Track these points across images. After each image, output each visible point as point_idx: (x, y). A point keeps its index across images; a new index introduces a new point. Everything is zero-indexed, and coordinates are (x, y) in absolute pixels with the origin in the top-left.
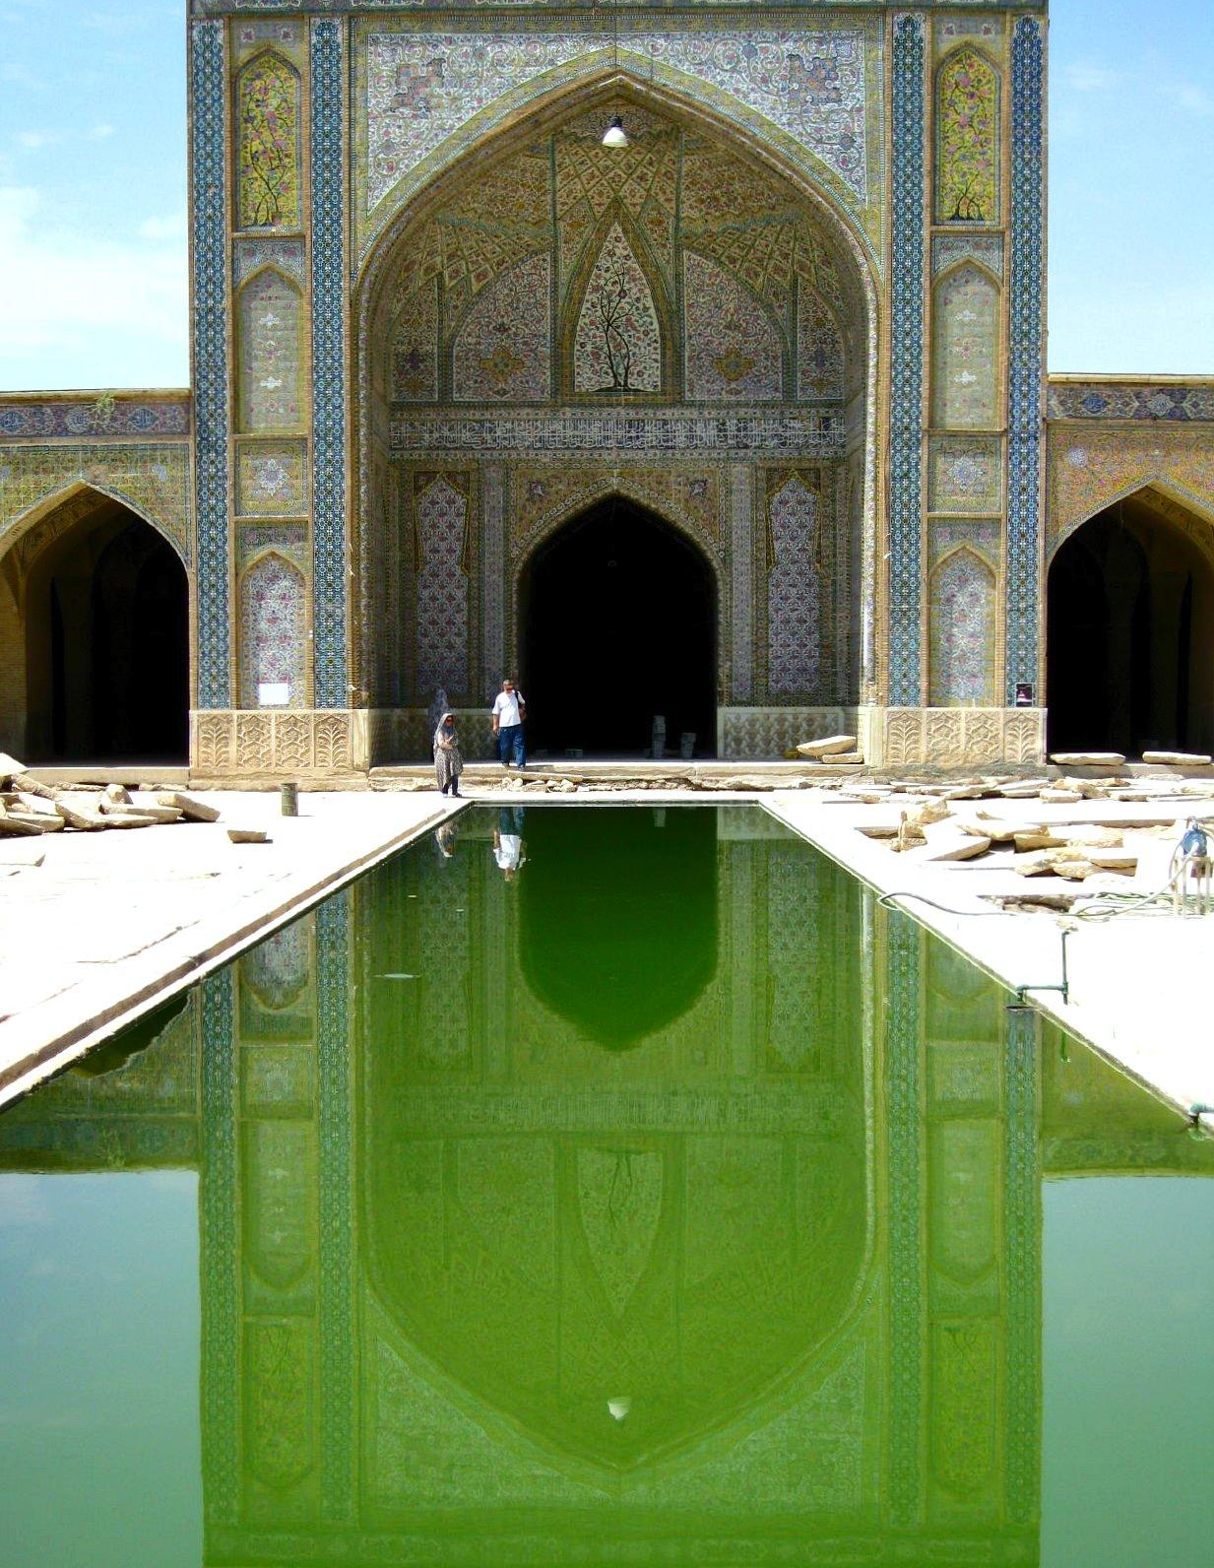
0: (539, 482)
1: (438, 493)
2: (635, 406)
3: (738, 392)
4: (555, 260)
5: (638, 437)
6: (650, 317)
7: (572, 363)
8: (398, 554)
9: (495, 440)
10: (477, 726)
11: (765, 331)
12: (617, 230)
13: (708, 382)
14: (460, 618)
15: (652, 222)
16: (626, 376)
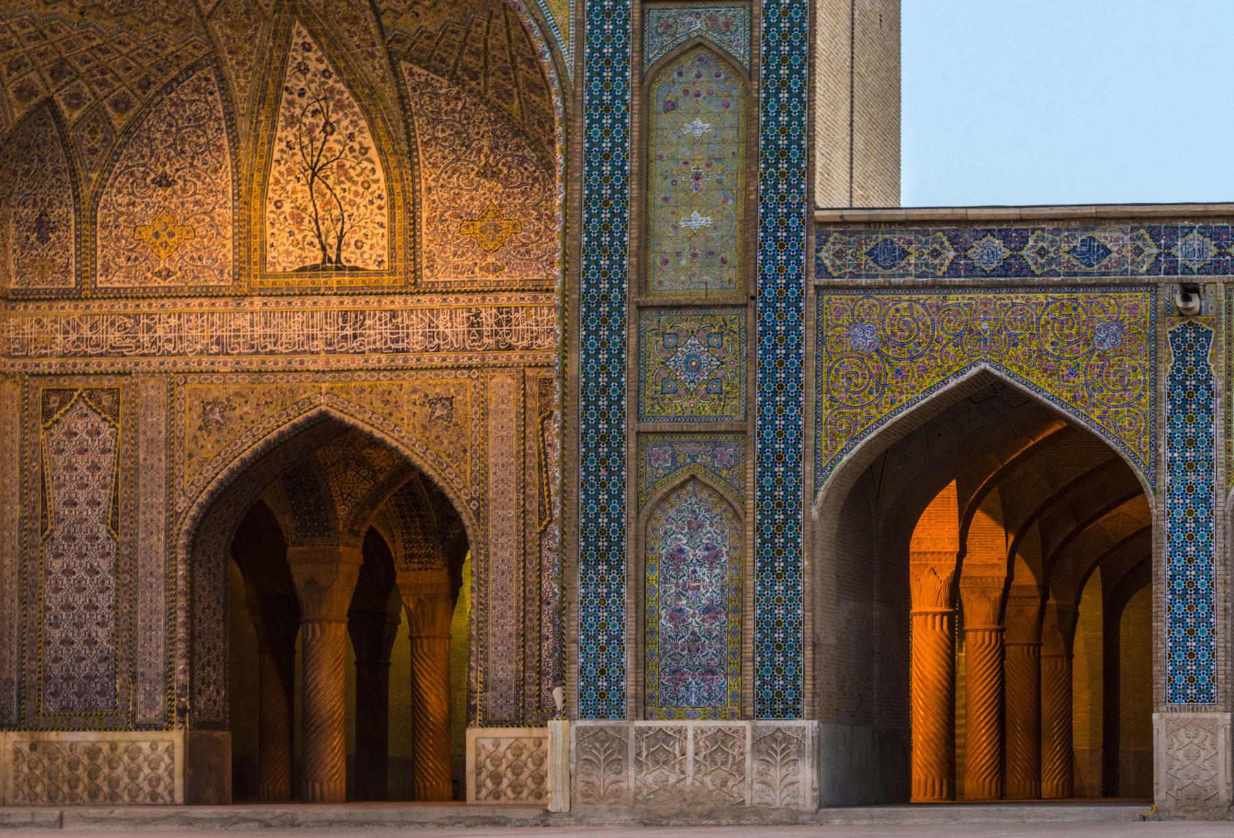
0: (215, 402)
1: (78, 421)
2: (353, 293)
3: (497, 269)
4: (222, 79)
5: (355, 337)
6: (372, 161)
7: (262, 231)
8: (17, 507)
9: (154, 343)
10: (126, 758)
11: (536, 180)
12: (300, 34)
13: (455, 254)
14: (104, 601)
15: (345, 19)
16: (339, 249)
